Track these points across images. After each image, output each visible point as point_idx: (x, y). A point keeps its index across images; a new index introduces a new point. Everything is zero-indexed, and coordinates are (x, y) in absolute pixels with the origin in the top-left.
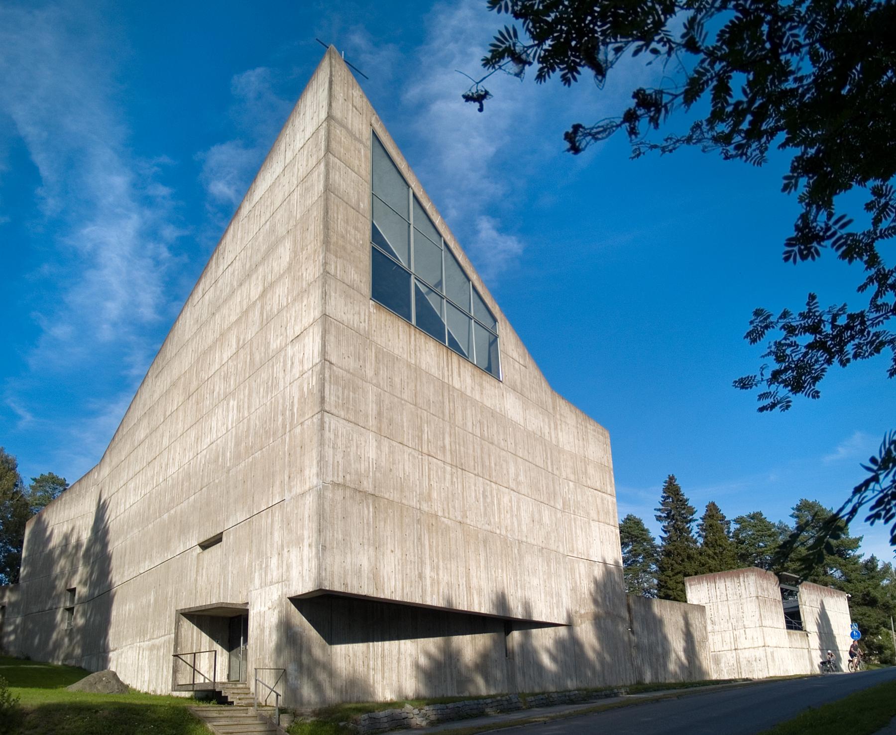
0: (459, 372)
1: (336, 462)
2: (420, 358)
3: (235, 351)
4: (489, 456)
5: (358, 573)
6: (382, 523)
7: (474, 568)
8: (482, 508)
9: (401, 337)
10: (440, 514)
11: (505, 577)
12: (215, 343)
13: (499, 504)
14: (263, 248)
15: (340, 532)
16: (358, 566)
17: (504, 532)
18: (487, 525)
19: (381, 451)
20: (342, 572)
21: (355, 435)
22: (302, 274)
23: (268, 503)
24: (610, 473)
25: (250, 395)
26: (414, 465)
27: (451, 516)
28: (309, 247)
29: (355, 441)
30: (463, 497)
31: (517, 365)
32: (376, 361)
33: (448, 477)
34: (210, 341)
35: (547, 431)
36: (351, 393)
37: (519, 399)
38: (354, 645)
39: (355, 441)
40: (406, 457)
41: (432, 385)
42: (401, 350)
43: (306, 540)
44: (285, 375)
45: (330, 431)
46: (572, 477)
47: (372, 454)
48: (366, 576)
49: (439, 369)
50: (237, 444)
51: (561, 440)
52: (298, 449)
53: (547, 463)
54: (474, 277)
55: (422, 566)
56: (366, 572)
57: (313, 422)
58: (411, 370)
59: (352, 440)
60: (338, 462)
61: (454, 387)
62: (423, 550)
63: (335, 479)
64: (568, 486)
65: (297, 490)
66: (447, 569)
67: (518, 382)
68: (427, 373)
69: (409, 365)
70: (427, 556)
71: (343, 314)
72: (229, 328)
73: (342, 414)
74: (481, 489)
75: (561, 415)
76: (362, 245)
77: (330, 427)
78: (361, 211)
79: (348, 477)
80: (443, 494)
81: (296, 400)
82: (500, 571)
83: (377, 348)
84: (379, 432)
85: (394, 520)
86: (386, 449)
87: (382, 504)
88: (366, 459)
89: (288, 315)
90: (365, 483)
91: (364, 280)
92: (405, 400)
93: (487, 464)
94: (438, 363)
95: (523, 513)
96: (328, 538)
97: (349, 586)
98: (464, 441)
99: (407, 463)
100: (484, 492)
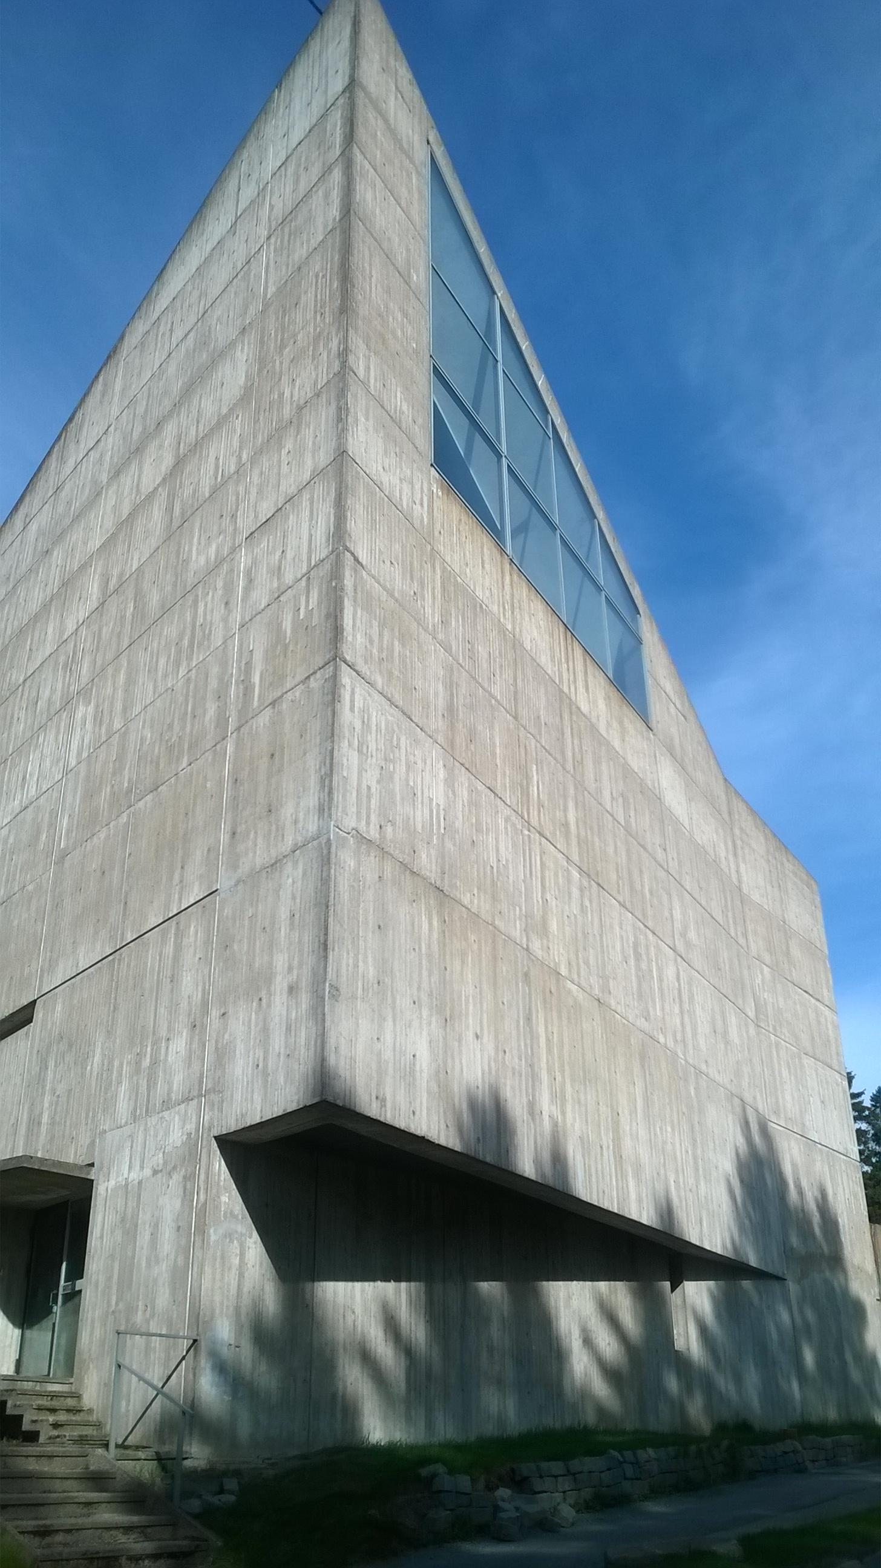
0: (586, 681)
1: (364, 787)
2: (521, 623)
3: (95, 605)
4: (641, 871)
5: (409, 1074)
6: (457, 964)
7: (626, 1112)
8: (634, 978)
9: (487, 566)
10: (564, 971)
11: (678, 1145)
12: (46, 607)
13: (661, 980)
14: (176, 388)
15: (370, 959)
16: (409, 1057)
17: (671, 1044)
18: (643, 1020)
19: (454, 792)
20: (374, 1066)
21: (403, 739)
22: (282, 394)
23: (167, 907)
24: (825, 963)
25: (130, 682)
26: (514, 845)
27: (583, 983)
28: (300, 337)
29: (403, 751)
30: (602, 946)
31: (672, 709)
32: (443, 595)
33: (575, 892)
34: (34, 606)
35: (723, 854)
36: (396, 643)
37: (680, 776)
38: (366, 1284)
39: (403, 751)
40: (501, 822)
41: (542, 690)
42: (487, 593)
43: (279, 978)
44: (230, 612)
45: (352, 709)
46: (767, 958)
47: (438, 793)
48: (425, 1084)
49: (553, 661)
50: (90, 795)
51: (745, 879)
52: (263, 763)
53: (727, 916)
54: (600, 514)
55: (533, 1086)
56: (425, 1075)
57: (309, 692)
58: (505, 640)
59: (398, 746)
60: (369, 788)
61: (579, 708)
62: (535, 1046)
63: (362, 827)
64: (762, 974)
65: (258, 854)
66: (579, 1103)
67: (677, 742)
68: (533, 659)
69: (502, 631)
70: (544, 1065)
71: (380, 468)
72: (84, 567)
73: (379, 681)
74: (632, 939)
75: (741, 829)
76: (416, 352)
77: (352, 701)
78: (413, 287)
79: (389, 829)
80: (567, 928)
81: (258, 657)
82: (669, 1129)
83: (444, 570)
84: (449, 749)
85: (480, 961)
86: (464, 793)
87: (456, 917)
88: (426, 801)
89: (241, 489)
90: (424, 856)
91: (420, 421)
92: (496, 700)
93: (638, 887)
94: (552, 649)
95: (699, 1011)
96: (344, 971)
97: (389, 1105)
98: (599, 825)
99: (502, 837)
100: (636, 945)
